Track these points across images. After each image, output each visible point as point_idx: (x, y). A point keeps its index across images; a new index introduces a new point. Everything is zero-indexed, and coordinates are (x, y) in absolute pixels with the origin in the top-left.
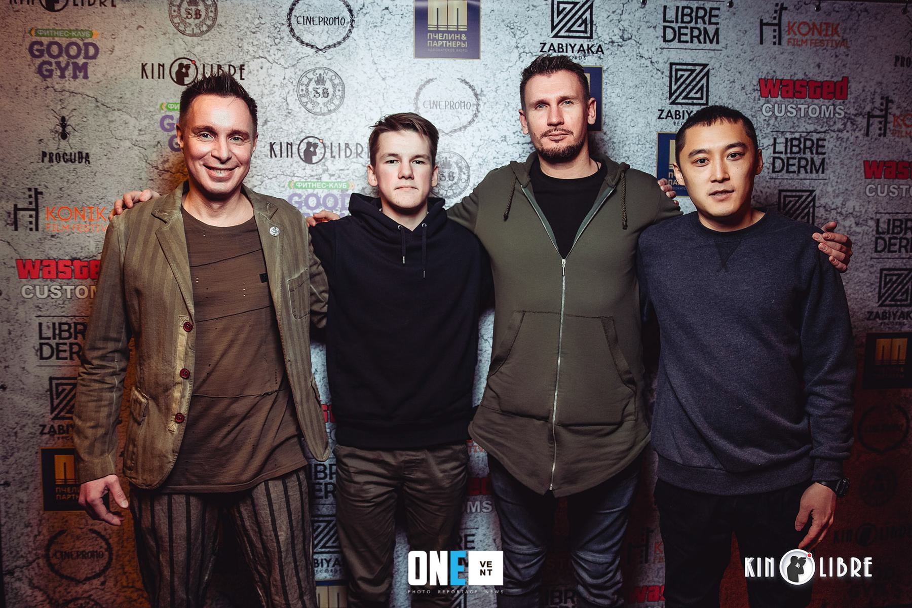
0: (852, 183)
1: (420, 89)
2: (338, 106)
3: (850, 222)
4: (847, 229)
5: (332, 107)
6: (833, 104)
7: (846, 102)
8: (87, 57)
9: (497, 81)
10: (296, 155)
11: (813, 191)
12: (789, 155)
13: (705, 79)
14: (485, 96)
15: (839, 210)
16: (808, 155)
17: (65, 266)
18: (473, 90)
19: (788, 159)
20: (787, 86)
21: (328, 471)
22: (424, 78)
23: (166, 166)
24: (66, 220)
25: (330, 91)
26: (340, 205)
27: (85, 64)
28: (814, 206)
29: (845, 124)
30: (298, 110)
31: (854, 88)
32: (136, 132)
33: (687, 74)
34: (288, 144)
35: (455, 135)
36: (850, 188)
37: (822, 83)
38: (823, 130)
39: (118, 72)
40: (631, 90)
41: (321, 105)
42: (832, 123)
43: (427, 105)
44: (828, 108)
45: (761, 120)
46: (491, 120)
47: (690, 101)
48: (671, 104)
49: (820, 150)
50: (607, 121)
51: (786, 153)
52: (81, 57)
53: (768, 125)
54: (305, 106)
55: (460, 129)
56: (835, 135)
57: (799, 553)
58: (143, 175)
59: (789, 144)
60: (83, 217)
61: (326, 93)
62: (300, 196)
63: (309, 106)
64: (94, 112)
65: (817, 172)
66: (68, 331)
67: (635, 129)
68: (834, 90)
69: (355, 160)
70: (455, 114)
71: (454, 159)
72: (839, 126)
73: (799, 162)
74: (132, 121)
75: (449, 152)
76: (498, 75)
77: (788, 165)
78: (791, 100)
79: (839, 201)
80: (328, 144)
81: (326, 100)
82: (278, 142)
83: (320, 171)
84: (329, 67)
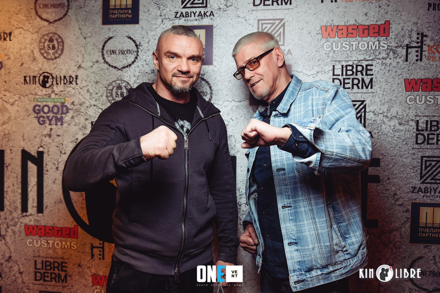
0: (395, 95)
1: (105, 43)
2: (60, 55)
3: (395, 122)
4: (392, 127)
5: (57, 55)
6: (378, 40)
7: (388, 38)
9: (149, 36)
10: (37, 83)
12: (345, 77)
13: (282, 29)
14: (142, 46)
15: (385, 115)
16: (359, 76)
18: (135, 42)
19: (344, 79)
21: (52, 266)
22: (107, 37)
25: (56, 46)
26: (60, 112)
28: (365, 112)
29: (388, 54)
30: (39, 57)
31: (394, 28)
34: (33, 76)
35: (124, 70)
36: (394, 99)
38: (370, 58)
41: (51, 54)
42: (377, 54)
43: (109, 52)
44: (374, 43)
46: (145, 61)
49: (369, 72)
50: (216, 58)
51: (342, 75)
53: (328, 57)
54: (43, 55)
55: (127, 66)
56: (380, 62)
59: (344, 69)
61: (54, 48)
62: (39, 106)
63: (45, 55)
65: (367, 87)
68: (381, 30)
69: (69, 85)
70: (125, 57)
71: (124, 84)
72: (384, 55)
75: (121, 80)
76: (149, 33)
77: (344, 83)
78: (345, 39)
79: (384, 108)
80: (55, 76)
81: (54, 51)
82: (28, 75)
83: (50, 92)
84: (56, 32)
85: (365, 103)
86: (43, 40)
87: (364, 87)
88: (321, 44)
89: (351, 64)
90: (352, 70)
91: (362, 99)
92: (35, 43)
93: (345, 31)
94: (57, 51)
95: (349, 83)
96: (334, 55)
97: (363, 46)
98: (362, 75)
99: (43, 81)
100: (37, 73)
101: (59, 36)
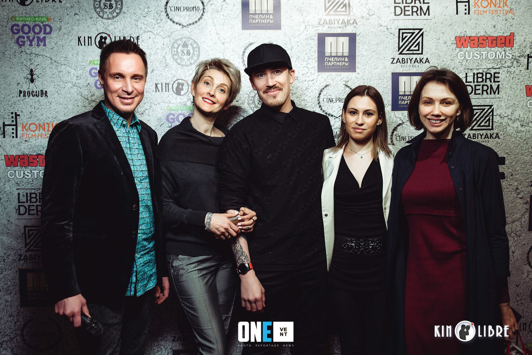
8: (45, 33)
10: (171, 90)
11: (492, 106)
12: (476, 84)
13: (420, 39)
16: (488, 83)
17: (33, 159)
19: (475, 86)
20: (474, 40)
23: (93, 98)
24: (34, 131)
25: (191, 51)
27: (44, 38)
28: (493, 115)
30: (172, 63)
32: (75, 78)
33: (409, 35)
37: (497, 37)
38: (498, 67)
39: (64, 42)
40: (374, 47)
41: (186, 60)
45: (457, 62)
47: (411, 52)
48: (400, 54)
49: (496, 80)
50: (359, 66)
51: (474, 82)
52: (42, 33)
53: (462, 65)
54: (176, 61)
57: (466, 323)
58: (80, 104)
59: (476, 76)
60: (44, 129)
61: (188, 53)
62: (173, 115)
63: (179, 61)
64: (50, 66)
65: (494, 93)
66: (35, 198)
67: (377, 70)
73: (483, 88)
74: (73, 71)
77: (476, 90)
78: (476, 49)
81: (189, 57)
85: (492, 108)
86: (176, 45)
87: (492, 93)
88: (456, 53)
89: (481, 72)
90: (482, 77)
91: (490, 104)
92: (166, 48)
93: (476, 41)
94: (192, 57)
95: (479, 89)
96: (467, 64)
97: (492, 55)
98: (491, 82)
99: (177, 88)
100: (170, 80)
101: (195, 41)
